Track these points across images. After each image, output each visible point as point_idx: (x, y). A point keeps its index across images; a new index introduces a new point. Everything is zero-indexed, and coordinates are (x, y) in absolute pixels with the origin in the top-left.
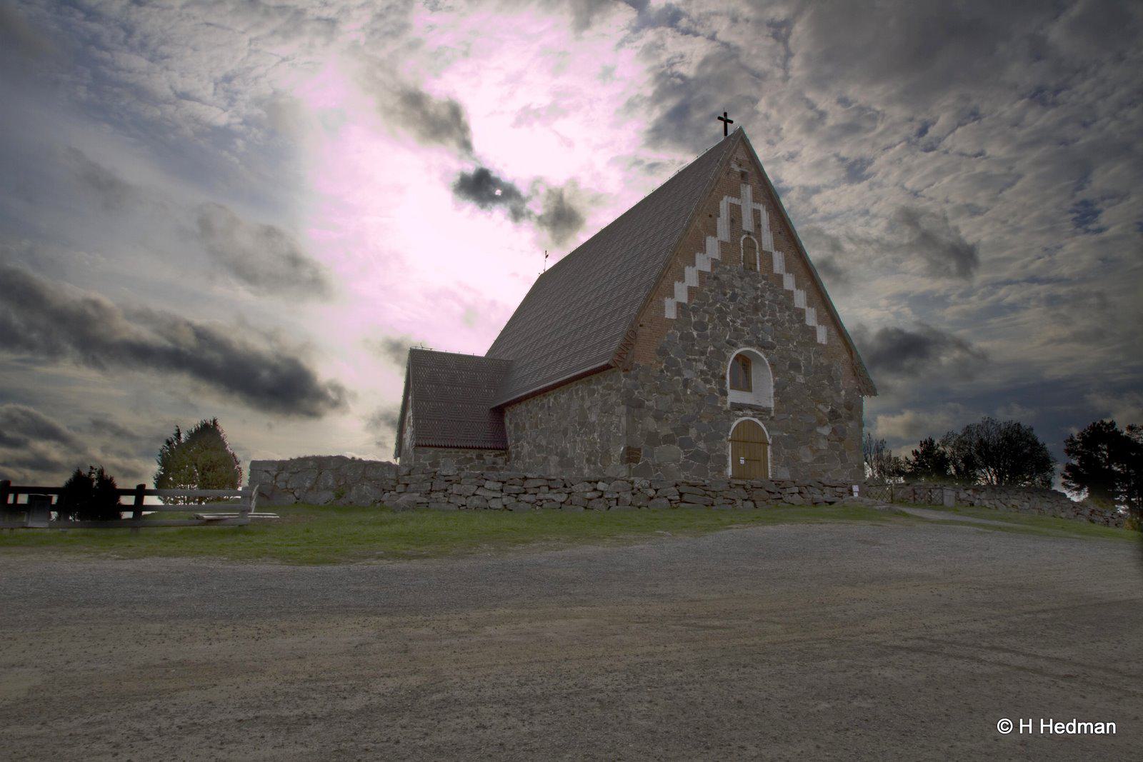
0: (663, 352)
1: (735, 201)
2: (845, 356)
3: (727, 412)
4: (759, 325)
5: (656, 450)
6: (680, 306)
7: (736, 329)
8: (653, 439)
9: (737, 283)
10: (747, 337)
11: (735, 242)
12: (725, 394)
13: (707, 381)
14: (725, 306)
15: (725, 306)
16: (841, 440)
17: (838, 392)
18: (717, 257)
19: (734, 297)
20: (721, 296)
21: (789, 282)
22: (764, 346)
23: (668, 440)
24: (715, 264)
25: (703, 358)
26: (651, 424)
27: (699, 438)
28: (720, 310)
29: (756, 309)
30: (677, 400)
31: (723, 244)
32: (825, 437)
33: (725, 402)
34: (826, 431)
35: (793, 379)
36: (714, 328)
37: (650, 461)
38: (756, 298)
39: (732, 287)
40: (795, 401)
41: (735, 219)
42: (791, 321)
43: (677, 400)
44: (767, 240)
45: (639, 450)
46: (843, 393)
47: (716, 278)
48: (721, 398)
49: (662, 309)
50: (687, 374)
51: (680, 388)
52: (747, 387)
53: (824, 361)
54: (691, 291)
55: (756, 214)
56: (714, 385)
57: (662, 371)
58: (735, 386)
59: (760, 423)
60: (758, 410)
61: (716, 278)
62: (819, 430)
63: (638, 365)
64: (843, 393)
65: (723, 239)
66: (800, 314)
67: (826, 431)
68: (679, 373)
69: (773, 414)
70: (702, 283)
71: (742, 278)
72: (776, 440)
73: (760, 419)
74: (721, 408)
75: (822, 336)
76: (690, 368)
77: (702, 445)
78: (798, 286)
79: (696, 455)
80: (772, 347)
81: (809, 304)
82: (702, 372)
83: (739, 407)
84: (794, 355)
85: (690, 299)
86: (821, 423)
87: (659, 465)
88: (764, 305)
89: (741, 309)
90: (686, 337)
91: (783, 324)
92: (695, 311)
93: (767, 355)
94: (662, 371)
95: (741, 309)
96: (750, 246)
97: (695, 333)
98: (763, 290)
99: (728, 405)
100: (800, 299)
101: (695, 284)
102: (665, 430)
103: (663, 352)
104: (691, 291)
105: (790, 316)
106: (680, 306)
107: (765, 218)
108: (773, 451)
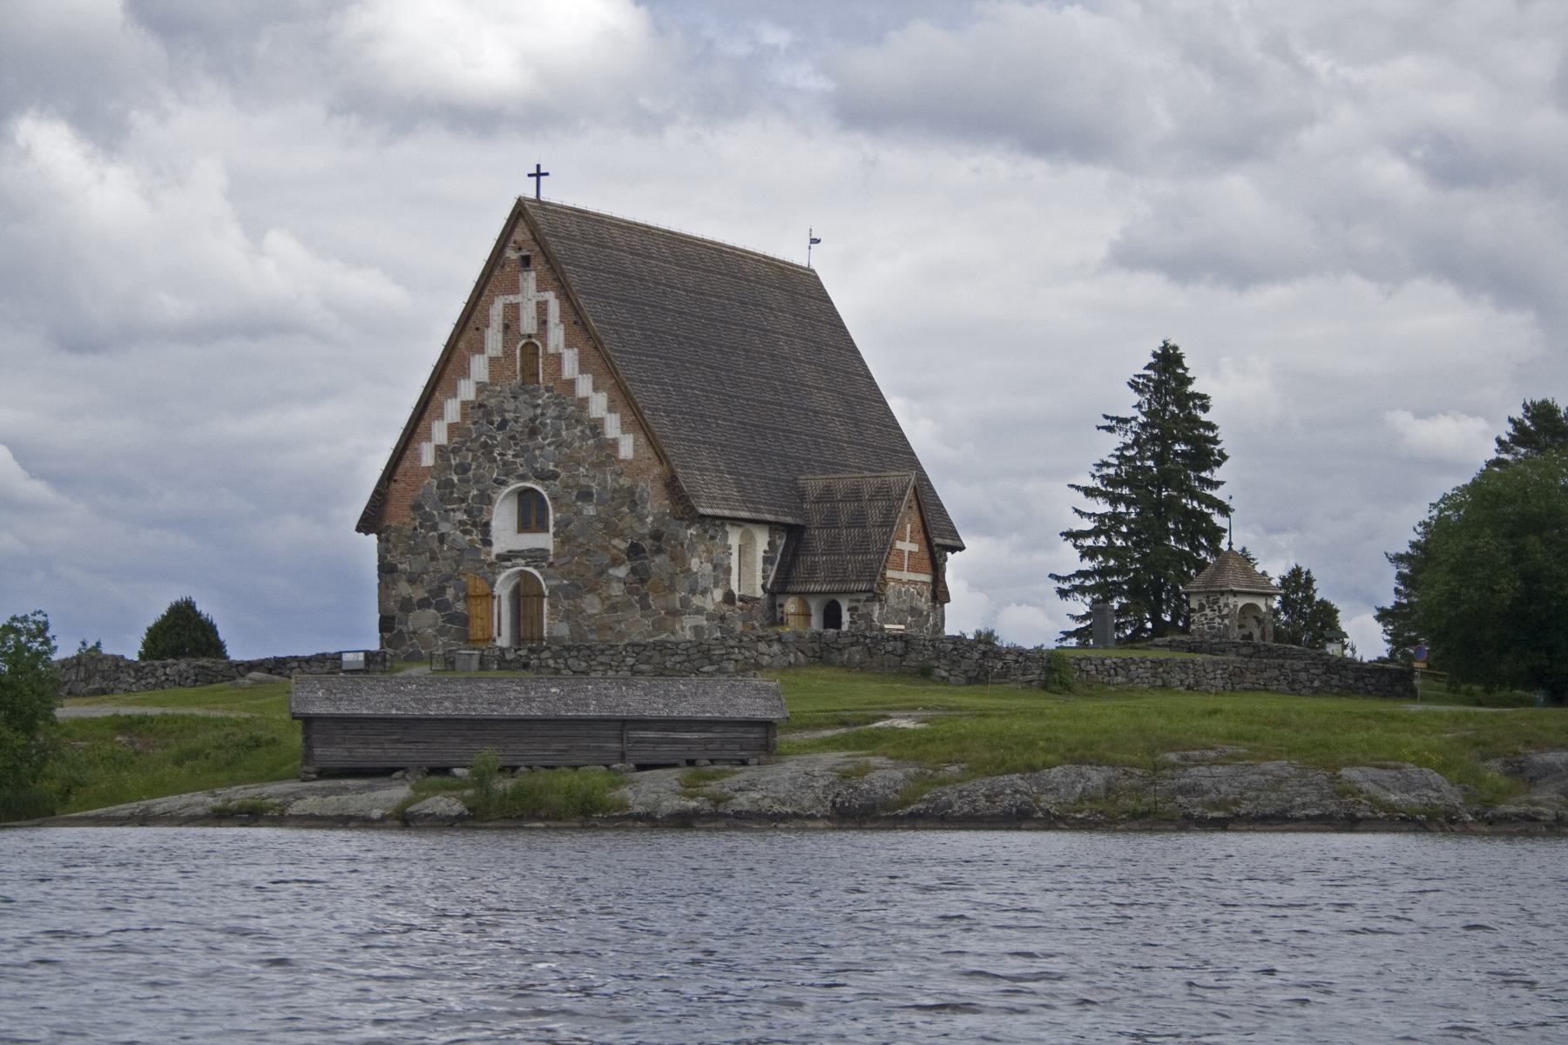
0: (417, 507)
2: (657, 470)
3: (490, 565)
6: (439, 448)
7: (505, 464)
8: (406, 605)
9: (510, 405)
10: (521, 470)
12: (487, 542)
13: (465, 532)
16: (643, 581)
17: (642, 519)
18: (485, 378)
19: (503, 425)
21: (584, 386)
22: (543, 476)
23: (424, 604)
24: (481, 388)
25: (464, 505)
26: (404, 589)
27: (457, 598)
28: (485, 445)
29: (533, 432)
30: (433, 558)
31: (493, 361)
32: (619, 580)
33: (489, 554)
34: (622, 572)
35: (579, 513)
36: (479, 466)
37: (405, 629)
38: (533, 420)
39: (502, 411)
40: (581, 540)
42: (583, 438)
43: (433, 558)
44: (556, 336)
45: (393, 618)
46: (650, 519)
49: (418, 457)
50: (444, 527)
51: (435, 545)
52: (543, 528)
53: (625, 482)
54: (452, 428)
55: (542, 308)
56: (476, 536)
58: (524, 526)
60: (536, 556)
61: (481, 406)
62: (611, 571)
64: (650, 519)
66: (596, 427)
67: (622, 572)
68: (434, 527)
69: (551, 559)
70: (464, 415)
72: (553, 592)
73: (536, 567)
74: (484, 561)
75: (627, 447)
76: (447, 520)
77: (460, 607)
78: (596, 389)
79: (452, 618)
80: (555, 476)
81: (610, 410)
82: (461, 522)
84: (583, 481)
85: (449, 439)
86: (616, 562)
87: (414, 633)
88: (544, 425)
89: (513, 438)
90: (447, 484)
91: (571, 444)
92: (455, 451)
93: (547, 488)
95: (513, 438)
96: (531, 351)
97: (455, 478)
98: (546, 406)
99: (493, 557)
100: (598, 405)
102: (419, 593)
103: (417, 507)
104: (452, 428)
107: (554, 308)
108: (550, 604)
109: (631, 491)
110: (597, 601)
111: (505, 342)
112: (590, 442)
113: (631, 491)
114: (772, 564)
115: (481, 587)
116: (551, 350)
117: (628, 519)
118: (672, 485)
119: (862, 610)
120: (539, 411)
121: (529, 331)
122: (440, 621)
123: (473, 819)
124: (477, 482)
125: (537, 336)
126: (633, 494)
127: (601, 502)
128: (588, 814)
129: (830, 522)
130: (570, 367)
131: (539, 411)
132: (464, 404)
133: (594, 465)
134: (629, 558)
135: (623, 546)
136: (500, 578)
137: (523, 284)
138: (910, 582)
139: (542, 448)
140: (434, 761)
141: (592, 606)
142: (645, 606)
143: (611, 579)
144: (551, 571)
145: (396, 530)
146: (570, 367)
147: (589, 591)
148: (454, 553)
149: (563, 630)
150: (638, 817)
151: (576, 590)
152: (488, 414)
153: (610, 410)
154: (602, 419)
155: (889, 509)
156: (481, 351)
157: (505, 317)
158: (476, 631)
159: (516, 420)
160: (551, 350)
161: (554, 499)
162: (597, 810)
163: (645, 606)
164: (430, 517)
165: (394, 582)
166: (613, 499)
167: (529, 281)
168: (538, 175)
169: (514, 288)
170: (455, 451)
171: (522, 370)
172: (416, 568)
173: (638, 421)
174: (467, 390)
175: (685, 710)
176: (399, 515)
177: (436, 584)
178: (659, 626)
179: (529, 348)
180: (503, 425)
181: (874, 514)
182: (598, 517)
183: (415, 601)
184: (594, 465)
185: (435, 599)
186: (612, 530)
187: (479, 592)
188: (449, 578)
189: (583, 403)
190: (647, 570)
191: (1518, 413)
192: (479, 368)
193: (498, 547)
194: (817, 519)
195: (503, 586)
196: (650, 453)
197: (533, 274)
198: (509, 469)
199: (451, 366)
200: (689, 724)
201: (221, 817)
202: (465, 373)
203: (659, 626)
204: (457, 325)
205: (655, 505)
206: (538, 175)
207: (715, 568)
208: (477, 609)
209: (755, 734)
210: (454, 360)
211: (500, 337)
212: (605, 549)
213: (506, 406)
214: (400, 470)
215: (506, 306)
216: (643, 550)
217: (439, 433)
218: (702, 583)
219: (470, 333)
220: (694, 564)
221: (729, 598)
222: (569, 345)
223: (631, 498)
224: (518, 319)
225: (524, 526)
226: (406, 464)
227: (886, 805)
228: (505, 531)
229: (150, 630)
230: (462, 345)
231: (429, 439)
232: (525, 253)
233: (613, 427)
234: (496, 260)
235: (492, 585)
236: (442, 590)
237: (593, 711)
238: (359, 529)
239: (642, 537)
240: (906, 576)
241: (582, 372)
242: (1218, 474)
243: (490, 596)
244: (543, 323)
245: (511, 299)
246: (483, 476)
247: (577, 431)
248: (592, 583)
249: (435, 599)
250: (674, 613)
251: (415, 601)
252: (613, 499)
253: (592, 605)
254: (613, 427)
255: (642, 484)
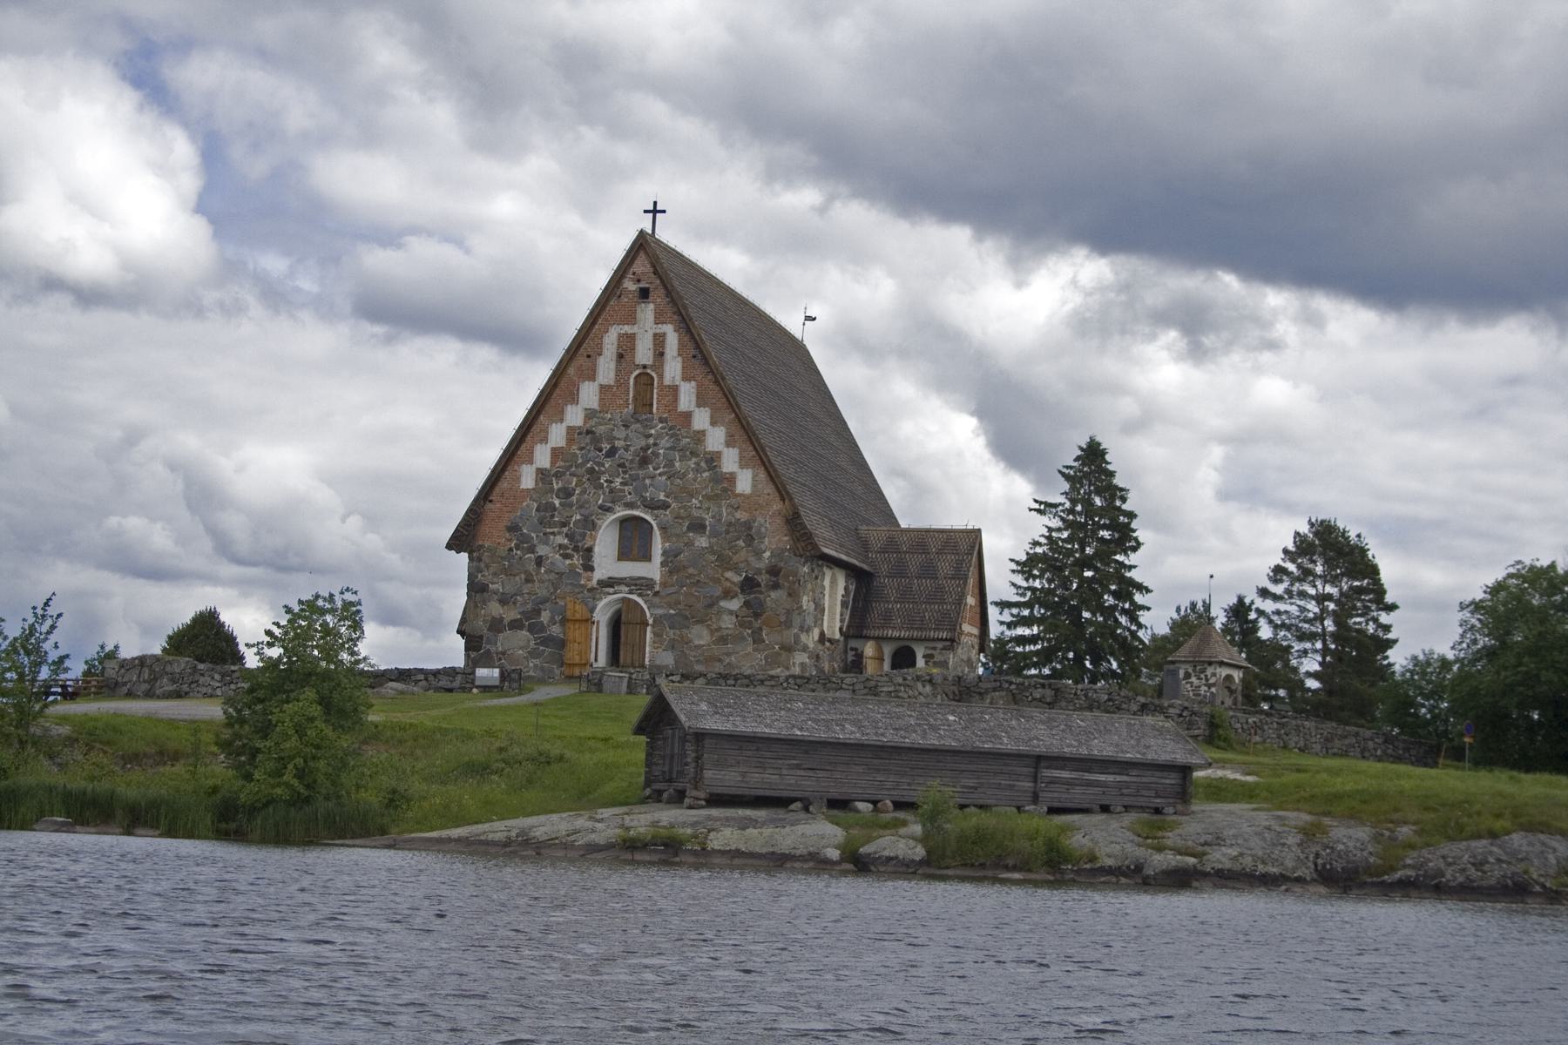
0: (513, 528)
1: (627, 329)
2: (777, 506)
3: (591, 590)
4: (648, 481)
5: (501, 636)
6: (540, 471)
8: (496, 626)
9: (620, 433)
11: (621, 381)
12: (589, 568)
13: (566, 556)
14: (599, 464)
15: (599, 464)
16: (757, 615)
17: (758, 554)
18: (595, 405)
19: (612, 452)
20: (592, 454)
21: (701, 419)
22: (652, 506)
23: (515, 625)
24: (590, 414)
25: (565, 530)
26: (495, 609)
28: (591, 471)
29: (644, 461)
30: (527, 581)
31: (604, 389)
32: (731, 612)
33: (590, 579)
34: (735, 605)
35: (690, 544)
36: (584, 492)
37: (493, 649)
39: (611, 439)
40: (691, 570)
41: (624, 354)
42: (698, 470)
43: (527, 581)
44: (673, 369)
45: (481, 637)
47: (588, 432)
48: (585, 575)
49: (518, 479)
50: (542, 550)
51: (532, 567)
52: (647, 557)
53: (742, 516)
54: (556, 453)
55: (659, 340)
56: (577, 561)
57: (511, 550)
58: (624, 554)
59: (640, 600)
60: (641, 585)
61: (588, 432)
63: (482, 546)
64: (768, 554)
65: (605, 382)
66: (713, 460)
67: (735, 605)
68: (532, 550)
69: (657, 588)
70: (570, 440)
71: (626, 426)
73: (640, 595)
75: (745, 482)
76: (546, 543)
77: (556, 630)
78: (713, 423)
79: (546, 641)
80: (665, 506)
81: (728, 444)
82: (560, 546)
83: (610, 583)
84: (695, 513)
85: (553, 463)
86: (728, 595)
87: (503, 653)
88: (656, 455)
89: (622, 465)
91: (684, 475)
92: (558, 475)
93: (657, 517)
94: (511, 550)
95: (622, 465)
96: (645, 381)
97: (557, 502)
98: (659, 436)
99: (594, 582)
100: (716, 439)
101: (562, 443)
102: (511, 614)
104: (556, 453)
105: (697, 464)
106: (541, 473)
107: (672, 340)
108: (654, 633)
109: (748, 526)
110: (705, 632)
111: (618, 372)
112: (706, 474)
113: (748, 526)
115: (580, 611)
116: (667, 381)
117: (743, 554)
118: (793, 521)
119: (938, 658)
120: (651, 441)
121: (644, 362)
122: (532, 643)
123: (936, 864)
124: (581, 507)
125: (653, 367)
126: (750, 528)
127: (715, 534)
128: (1057, 867)
129: (899, 572)
130: (687, 397)
131: (651, 441)
132: (570, 429)
133: (708, 498)
134: (743, 591)
135: (737, 579)
136: (601, 604)
137: (639, 315)
139: (653, 477)
140: (835, 793)
141: (701, 637)
142: (757, 640)
143: (720, 612)
144: (656, 600)
145: (489, 550)
146: (687, 397)
147: (698, 622)
148: (552, 576)
149: (667, 659)
150: (1110, 871)
151: (684, 619)
152: (596, 441)
153: (728, 444)
154: (719, 454)
155: (959, 563)
156: (592, 378)
157: (619, 347)
158: (572, 654)
159: (626, 450)
160: (667, 381)
161: (663, 529)
162: (1067, 861)
163: (757, 640)
164: (527, 539)
165: (484, 602)
166: (727, 532)
167: (647, 312)
168: (655, 211)
169: (631, 319)
170: (558, 475)
171: (635, 399)
172: (509, 589)
173: (759, 456)
174: (574, 416)
175: (1101, 748)
176: (493, 534)
177: (529, 607)
178: (773, 661)
179: (644, 379)
180: (612, 452)
181: (945, 566)
182: (710, 549)
183: (506, 622)
184: (708, 498)
185: (529, 621)
186: (725, 563)
187: (578, 616)
188: (545, 601)
189: (700, 436)
190: (761, 604)
191: (1304, 529)
192: (589, 394)
193: (600, 574)
194: (884, 569)
195: (603, 612)
196: (770, 489)
197: (652, 306)
198: (615, 497)
199: (558, 391)
200: (1106, 764)
201: (630, 850)
202: (573, 398)
203: (773, 661)
204: (568, 351)
205: (774, 540)
206: (655, 211)
208: (575, 632)
209: (1171, 780)
210: (562, 384)
211: (613, 365)
212: (717, 581)
213: (615, 434)
214: (497, 490)
215: (620, 336)
216: (759, 585)
217: (543, 457)
219: (580, 360)
222: (686, 378)
223: (748, 533)
224: (633, 349)
225: (624, 554)
226: (503, 485)
227: (1369, 870)
228: (606, 560)
229: (170, 637)
230: (571, 371)
231: (531, 462)
232: (642, 285)
233: (730, 461)
234: (613, 288)
235: (592, 611)
236: (538, 612)
237: (1007, 744)
238: (449, 546)
239: (759, 571)
241: (699, 406)
242: (1133, 559)
243: (589, 621)
244: (660, 354)
245: (627, 329)
246: (587, 502)
247: (692, 463)
248: (704, 613)
249: (529, 621)
250: (788, 649)
251: (506, 622)
252: (727, 532)
253: (700, 636)
254: (730, 461)
255: (760, 519)
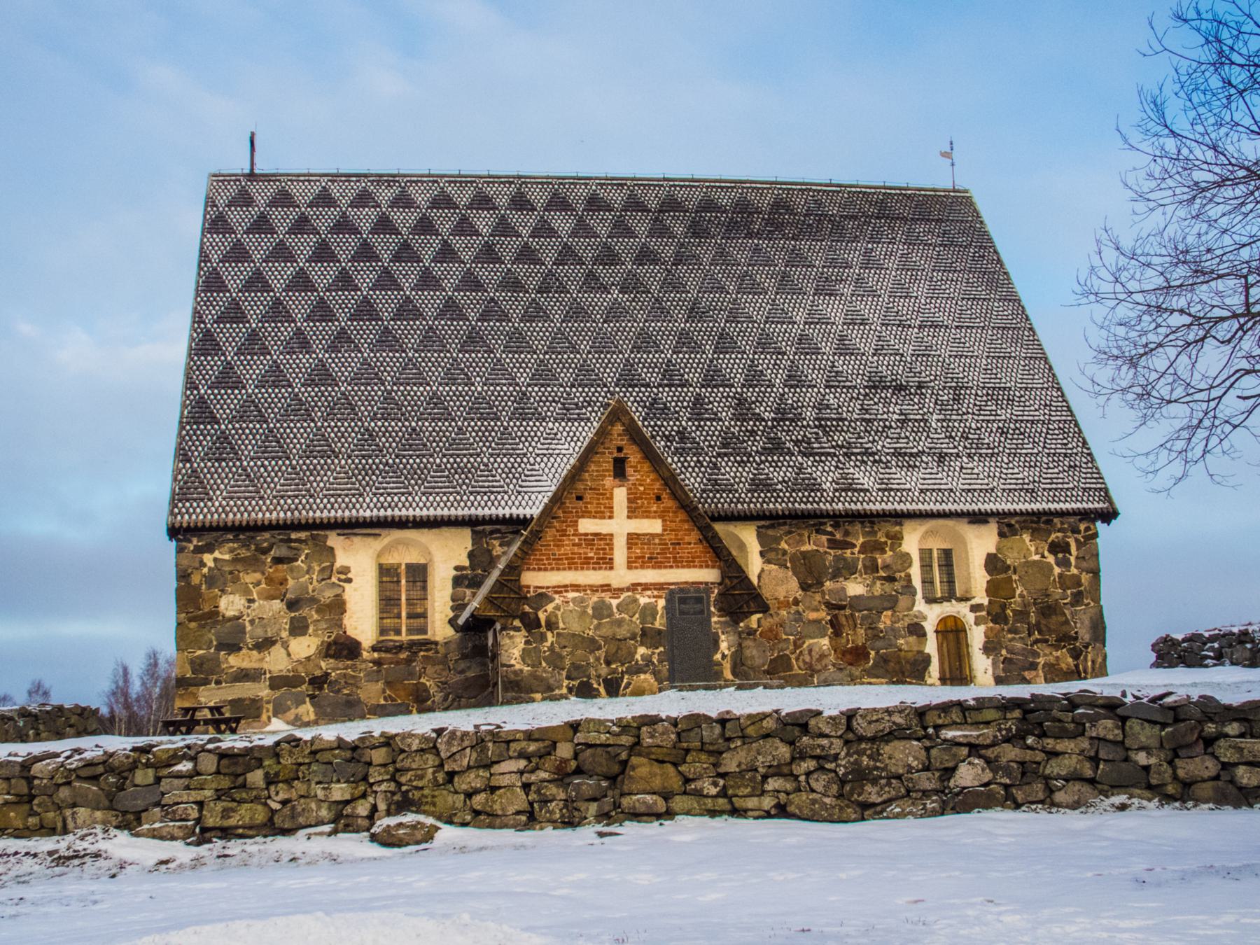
114: (475, 583)
138: (634, 587)
207: (292, 605)
218: (252, 633)
220: (230, 604)
221: (345, 648)
240: (621, 576)
